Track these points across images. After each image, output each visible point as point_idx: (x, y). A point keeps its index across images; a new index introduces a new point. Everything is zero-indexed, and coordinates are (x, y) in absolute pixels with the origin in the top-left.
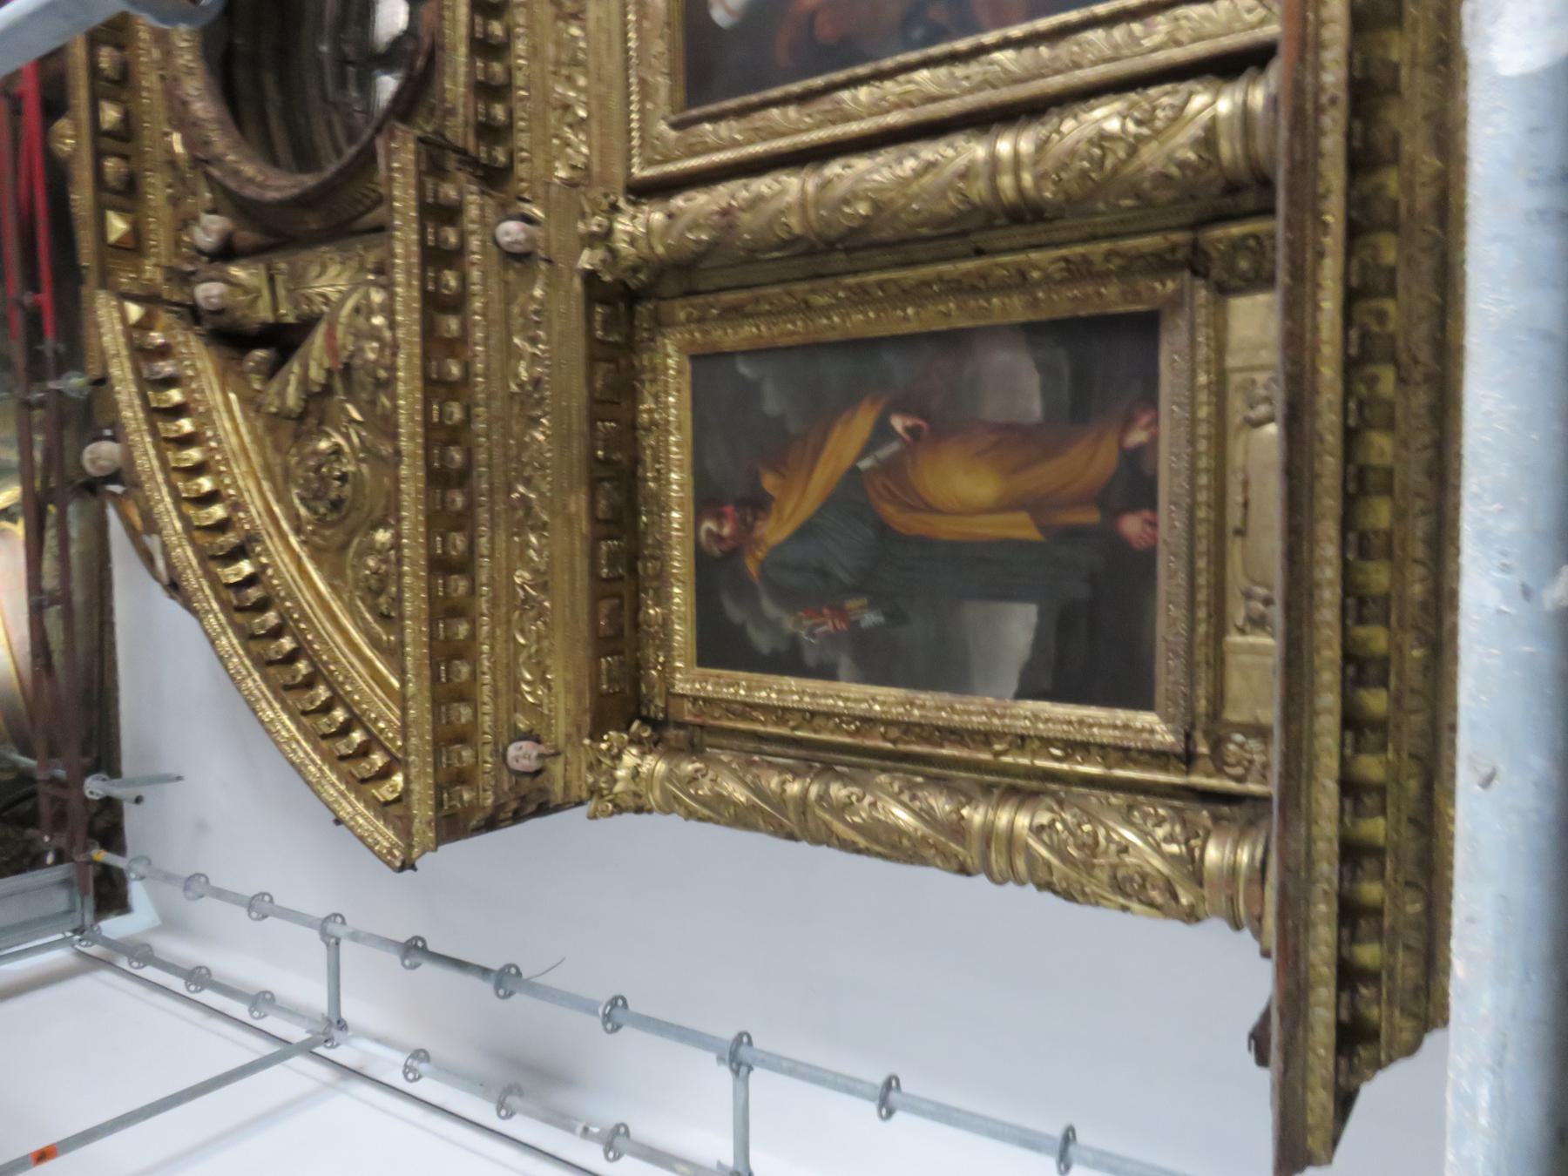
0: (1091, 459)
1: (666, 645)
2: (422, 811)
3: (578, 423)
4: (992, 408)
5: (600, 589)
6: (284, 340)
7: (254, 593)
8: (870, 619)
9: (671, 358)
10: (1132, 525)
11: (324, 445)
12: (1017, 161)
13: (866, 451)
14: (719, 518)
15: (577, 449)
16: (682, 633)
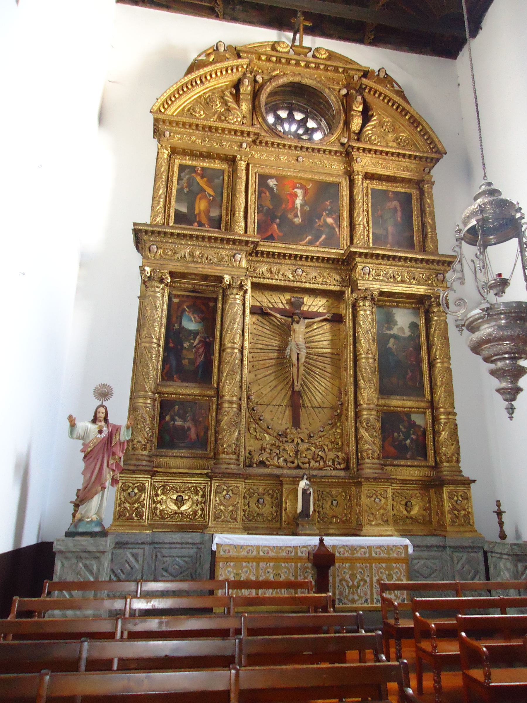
0: (204, 220)
1: (182, 159)
2: (160, 116)
3: (216, 152)
4: (211, 210)
5: (192, 151)
6: (237, 97)
7: (194, 84)
8: (185, 191)
9: (224, 166)
10: (196, 224)
11: (218, 103)
12: (239, 214)
13: (208, 193)
14: (201, 171)
15: (212, 151)
16: (184, 162)
